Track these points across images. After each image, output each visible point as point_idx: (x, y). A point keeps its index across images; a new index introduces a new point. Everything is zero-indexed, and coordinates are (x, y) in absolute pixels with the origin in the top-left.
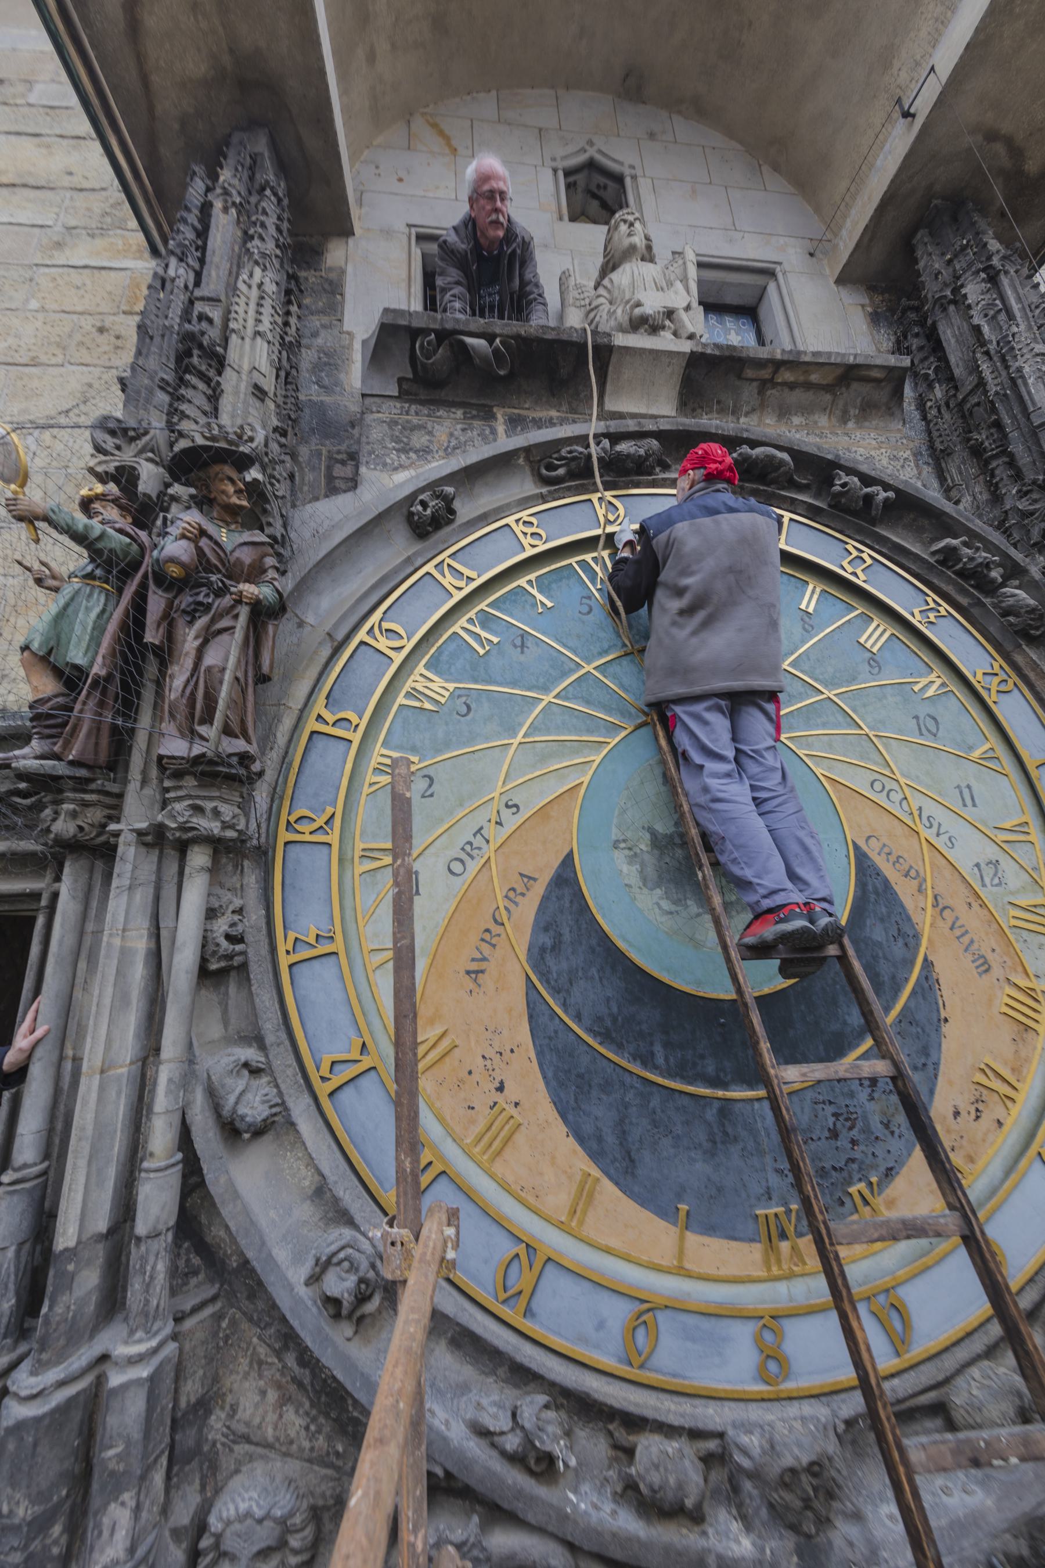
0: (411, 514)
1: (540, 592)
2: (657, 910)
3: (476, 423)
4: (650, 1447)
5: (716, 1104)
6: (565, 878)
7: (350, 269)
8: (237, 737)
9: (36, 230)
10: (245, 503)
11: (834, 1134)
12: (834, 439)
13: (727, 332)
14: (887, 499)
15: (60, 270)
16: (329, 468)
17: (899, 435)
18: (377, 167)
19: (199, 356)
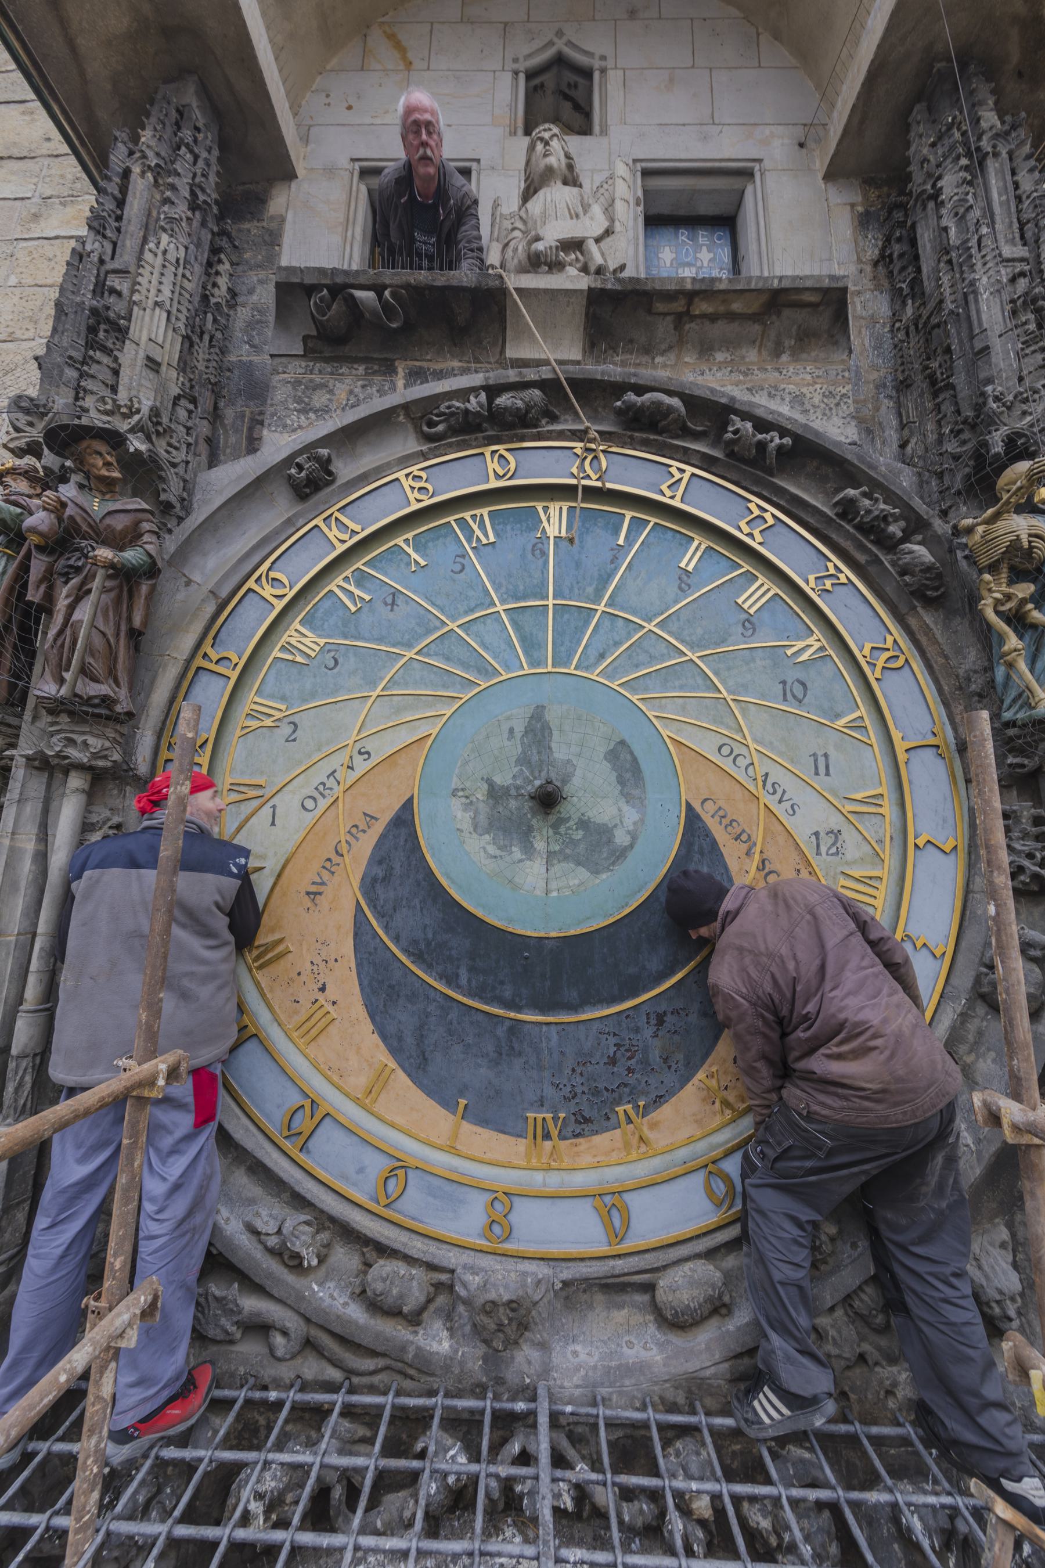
0: (290, 476)
1: (416, 550)
2: (482, 854)
3: (377, 379)
4: (384, 1267)
5: (508, 1023)
6: (404, 821)
7: (290, 217)
8: (95, 680)
9: (18, 203)
10: (116, 474)
11: (613, 1061)
12: (762, 375)
13: (698, 248)
14: (780, 448)
15: (36, 243)
16: (250, 429)
17: (841, 367)
18: (328, 96)
19: (106, 331)
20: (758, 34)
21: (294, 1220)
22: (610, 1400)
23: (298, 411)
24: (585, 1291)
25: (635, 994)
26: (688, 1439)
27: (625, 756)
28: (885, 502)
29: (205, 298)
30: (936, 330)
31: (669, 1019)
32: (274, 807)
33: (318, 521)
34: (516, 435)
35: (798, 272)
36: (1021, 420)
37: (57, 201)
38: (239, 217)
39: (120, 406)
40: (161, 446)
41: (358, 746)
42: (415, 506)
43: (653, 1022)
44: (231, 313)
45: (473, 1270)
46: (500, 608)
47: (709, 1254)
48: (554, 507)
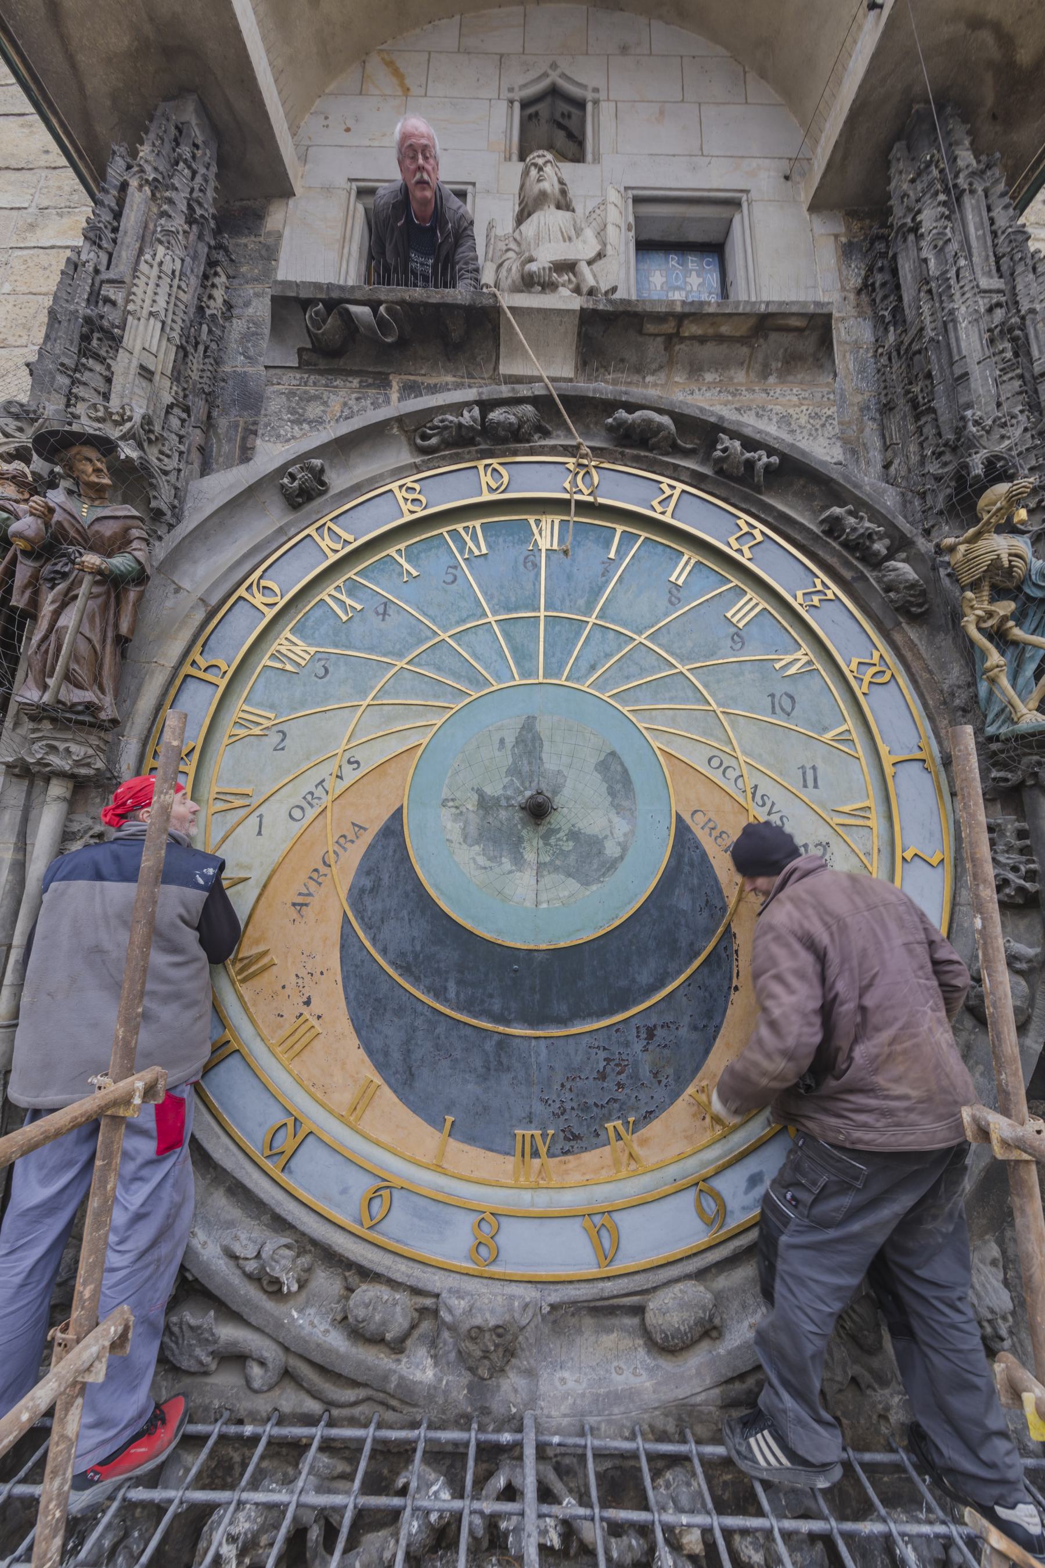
0: (282, 486)
1: (408, 561)
3: (372, 392)
4: (367, 1292)
5: (496, 1037)
6: (393, 831)
7: (287, 233)
8: (79, 686)
9: (14, 213)
10: (106, 481)
11: (602, 1076)
12: (749, 396)
13: (687, 273)
14: (767, 466)
15: (31, 252)
16: (244, 439)
17: (826, 390)
18: (326, 118)
19: (99, 339)
20: (745, 73)
21: (274, 1243)
22: (598, 1429)
23: (292, 422)
24: (573, 1315)
25: (625, 1007)
26: (678, 1469)
27: (615, 767)
28: (870, 521)
29: (201, 310)
30: (917, 357)
31: (659, 1032)
32: (261, 816)
33: (311, 530)
34: (509, 449)
35: (784, 298)
36: (1000, 443)
37: (54, 211)
38: (236, 232)
39: (111, 414)
40: (152, 454)
41: (347, 755)
42: (408, 518)
43: (644, 1036)
44: (227, 324)
45: (459, 1294)
46: (491, 619)
47: (700, 1275)
48: (546, 520)
